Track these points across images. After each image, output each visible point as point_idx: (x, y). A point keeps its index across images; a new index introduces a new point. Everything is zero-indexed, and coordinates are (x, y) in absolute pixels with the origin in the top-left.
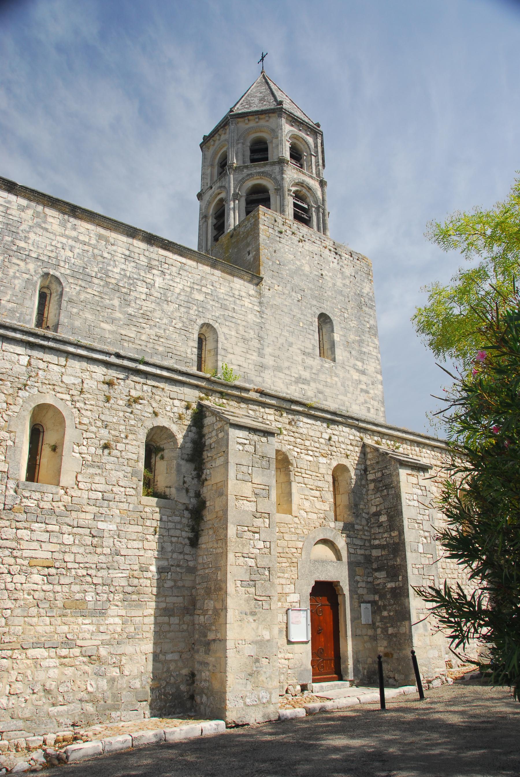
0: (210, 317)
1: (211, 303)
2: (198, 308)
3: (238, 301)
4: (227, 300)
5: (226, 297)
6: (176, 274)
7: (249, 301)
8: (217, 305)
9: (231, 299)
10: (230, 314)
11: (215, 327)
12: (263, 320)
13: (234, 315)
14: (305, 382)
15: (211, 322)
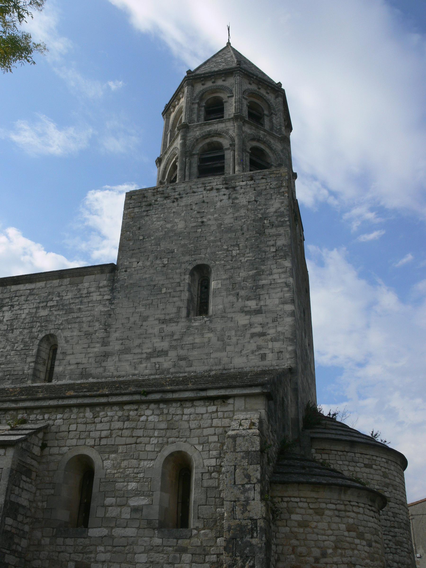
0: (53, 327)
1: (55, 313)
2: (41, 323)
3: (85, 300)
4: (73, 303)
5: (71, 301)
6: (24, 302)
7: (98, 293)
8: (61, 313)
9: (77, 301)
10: (75, 315)
11: (57, 334)
12: (113, 307)
13: (79, 315)
14: (164, 353)
15: (52, 332)
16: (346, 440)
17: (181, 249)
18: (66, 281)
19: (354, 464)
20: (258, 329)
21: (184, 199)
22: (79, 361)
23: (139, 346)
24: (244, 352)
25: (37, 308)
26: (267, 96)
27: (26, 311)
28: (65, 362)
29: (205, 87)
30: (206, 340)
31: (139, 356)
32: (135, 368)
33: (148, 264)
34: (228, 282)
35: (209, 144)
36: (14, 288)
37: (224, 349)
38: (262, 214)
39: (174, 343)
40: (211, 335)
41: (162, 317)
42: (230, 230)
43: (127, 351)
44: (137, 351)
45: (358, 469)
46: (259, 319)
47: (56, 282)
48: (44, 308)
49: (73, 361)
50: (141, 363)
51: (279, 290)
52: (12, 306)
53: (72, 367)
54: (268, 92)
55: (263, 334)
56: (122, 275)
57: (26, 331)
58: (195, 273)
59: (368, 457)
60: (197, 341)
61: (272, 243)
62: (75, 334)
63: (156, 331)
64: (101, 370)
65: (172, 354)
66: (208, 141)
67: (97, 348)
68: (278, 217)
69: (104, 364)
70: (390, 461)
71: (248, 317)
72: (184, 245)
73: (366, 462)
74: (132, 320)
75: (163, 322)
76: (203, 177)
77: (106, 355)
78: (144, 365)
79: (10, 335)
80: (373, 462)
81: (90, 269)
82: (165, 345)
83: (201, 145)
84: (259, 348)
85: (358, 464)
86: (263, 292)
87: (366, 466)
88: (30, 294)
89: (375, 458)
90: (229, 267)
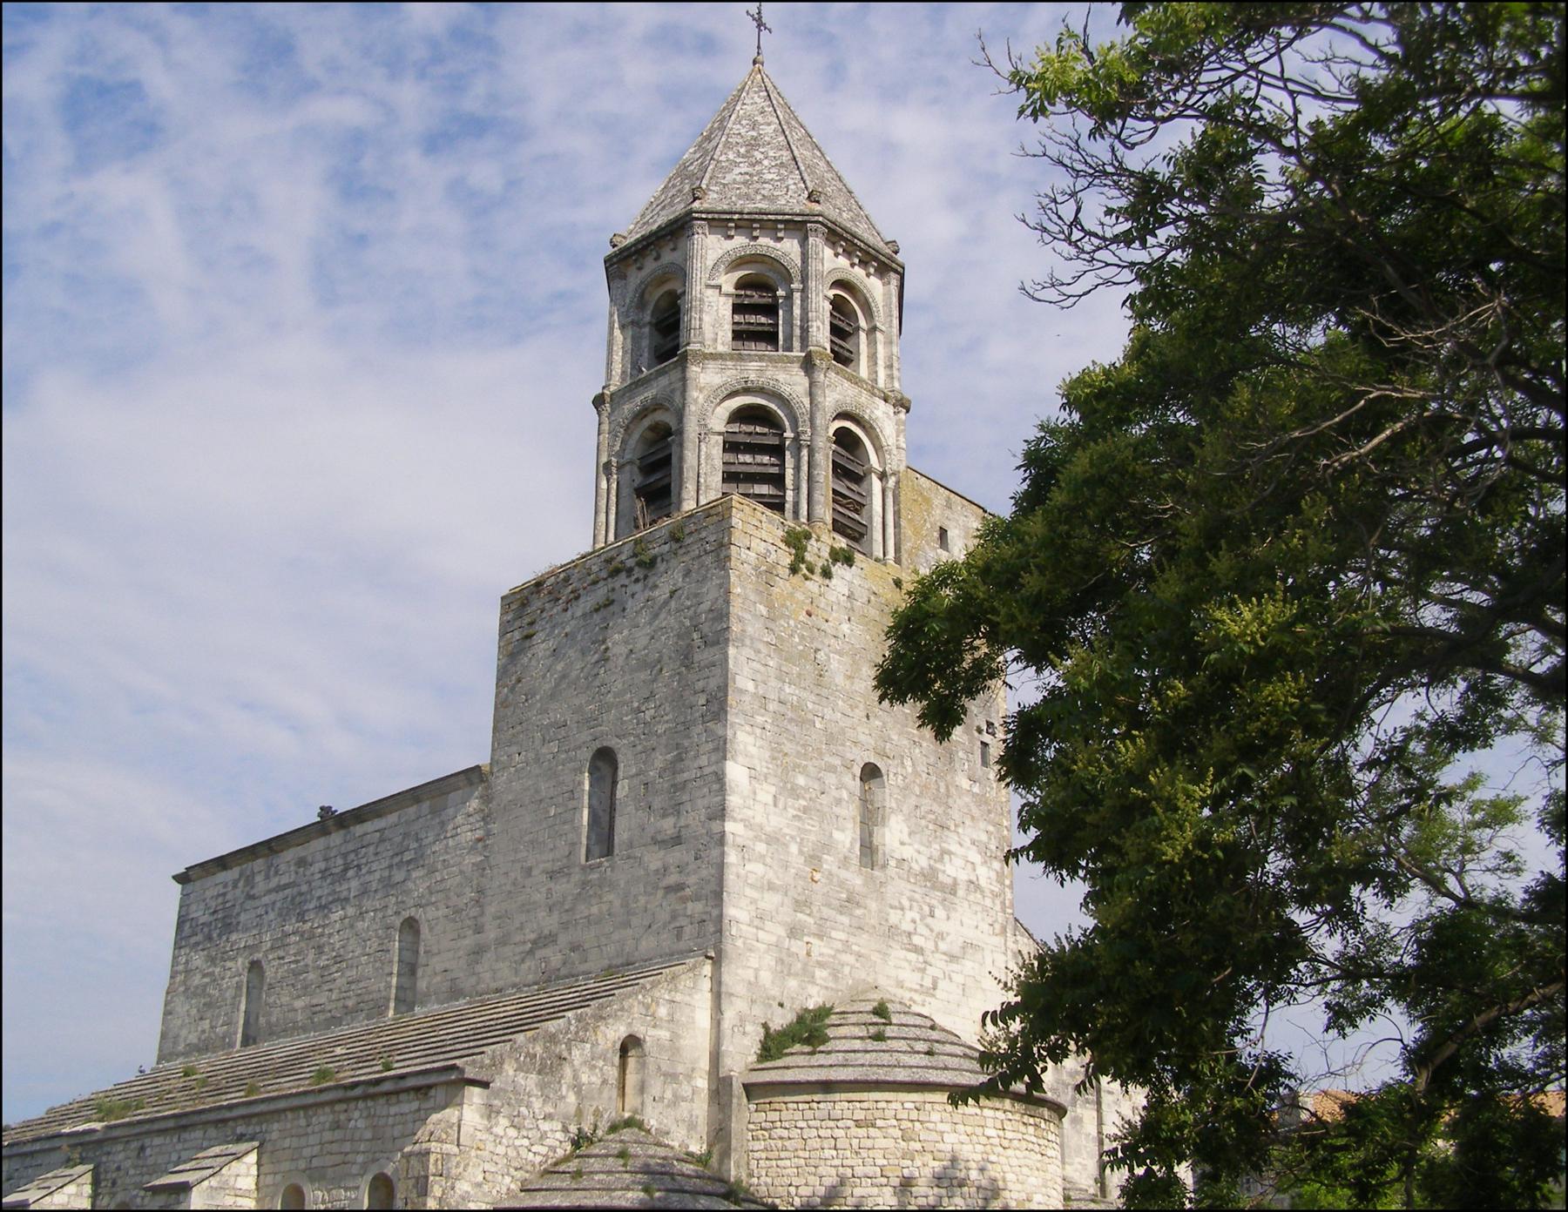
15: (413, 912)
16: (809, 1083)
17: (576, 718)
18: (426, 806)
19: (832, 1124)
20: (672, 879)
21: (582, 600)
22: (447, 966)
23: (521, 928)
24: (654, 927)
25: (390, 867)
26: (778, 245)
27: (377, 875)
28: (429, 970)
29: (644, 273)
30: (605, 907)
31: (521, 948)
32: (517, 973)
33: (531, 755)
34: (636, 781)
35: (653, 428)
36: (358, 830)
37: (627, 924)
38: (691, 619)
39: (565, 918)
40: (611, 897)
41: (548, 866)
42: (644, 664)
43: (503, 941)
44: (518, 938)
45: (839, 1133)
46: (676, 855)
47: (412, 810)
48: (400, 865)
49: (439, 968)
50: (523, 961)
51: (706, 790)
52: (358, 866)
53: (439, 978)
54: (780, 235)
55: (680, 887)
56: (500, 781)
57: (380, 915)
58: (600, 764)
59: (865, 1105)
60: (595, 910)
61: (700, 684)
62: (440, 913)
63: (539, 897)
64: (473, 980)
65: (563, 939)
66: (647, 422)
67: (469, 941)
68: (714, 619)
69: (479, 968)
70: (928, 1106)
71: (662, 853)
72: (578, 710)
73: (860, 1115)
74: (512, 875)
75: (551, 875)
76: (681, 487)
77: (478, 952)
78: (528, 964)
79: (360, 925)
80: (878, 1114)
81: (452, 780)
82: (550, 922)
83: (636, 436)
84: (674, 917)
85: (840, 1124)
86: (685, 798)
87: (858, 1124)
88: (382, 840)
89: (880, 1105)
90: (639, 748)
